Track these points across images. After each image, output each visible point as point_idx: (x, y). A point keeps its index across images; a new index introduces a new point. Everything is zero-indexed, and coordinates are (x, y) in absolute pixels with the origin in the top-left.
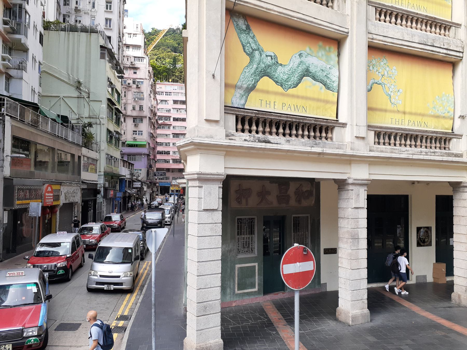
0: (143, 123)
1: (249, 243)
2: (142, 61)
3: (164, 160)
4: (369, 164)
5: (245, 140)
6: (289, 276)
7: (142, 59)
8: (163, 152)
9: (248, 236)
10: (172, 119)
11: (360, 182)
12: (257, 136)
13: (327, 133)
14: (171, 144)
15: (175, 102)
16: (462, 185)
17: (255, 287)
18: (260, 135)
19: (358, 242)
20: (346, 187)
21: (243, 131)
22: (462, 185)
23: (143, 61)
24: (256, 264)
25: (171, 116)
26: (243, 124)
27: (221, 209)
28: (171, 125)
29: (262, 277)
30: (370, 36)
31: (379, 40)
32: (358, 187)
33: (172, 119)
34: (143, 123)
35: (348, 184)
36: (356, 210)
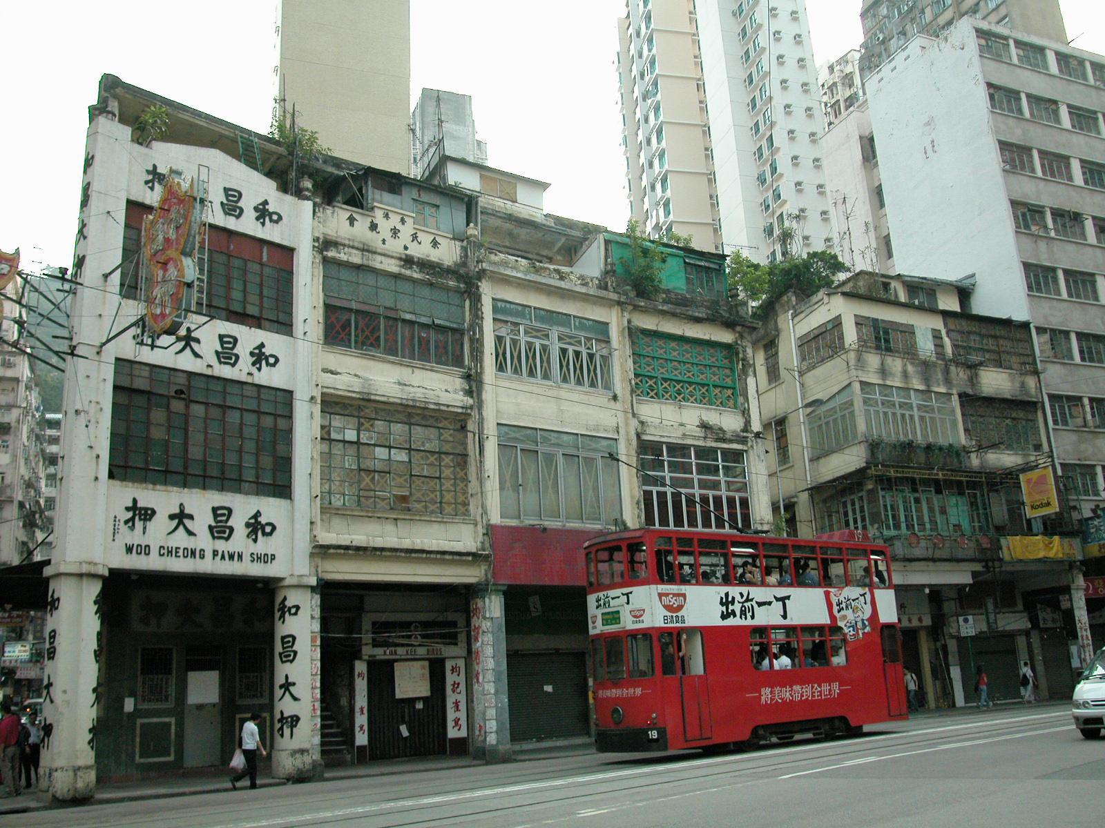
1: (161, 688)
9: (160, 676)
17: (169, 755)
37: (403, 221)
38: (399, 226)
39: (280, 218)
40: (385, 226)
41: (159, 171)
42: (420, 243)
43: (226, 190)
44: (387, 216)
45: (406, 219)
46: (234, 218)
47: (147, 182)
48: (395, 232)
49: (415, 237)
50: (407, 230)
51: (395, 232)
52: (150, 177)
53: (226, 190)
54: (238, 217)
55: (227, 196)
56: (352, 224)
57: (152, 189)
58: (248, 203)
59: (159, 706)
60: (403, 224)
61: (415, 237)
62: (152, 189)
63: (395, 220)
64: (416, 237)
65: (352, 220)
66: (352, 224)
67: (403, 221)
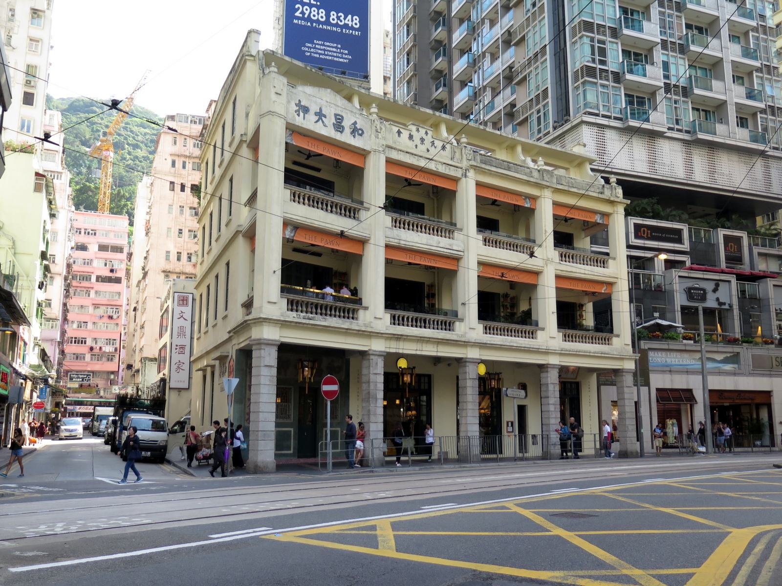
0: (52, 285)
2: (57, 179)
3: (74, 354)
4: (385, 340)
5: (294, 317)
6: (326, 392)
7: (58, 176)
8: (74, 340)
10: (94, 278)
11: (378, 353)
12: (302, 314)
13: (353, 314)
14: (89, 324)
15: (103, 248)
16: (463, 360)
17: (290, 450)
18: (304, 314)
19: (376, 400)
20: (368, 357)
21: (292, 310)
22: (463, 360)
23: (60, 179)
24: (292, 430)
25: (93, 273)
26: (292, 306)
27: (276, 366)
28: (92, 288)
29: (297, 442)
30: (387, 239)
31: (394, 242)
32: (376, 357)
33: (94, 278)
34: (52, 285)
35: (369, 354)
36: (375, 376)
37: (426, 133)
38: (424, 136)
39: (363, 132)
40: (417, 136)
41: (302, 104)
42: (435, 147)
43: (336, 115)
44: (418, 130)
45: (428, 132)
46: (339, 133)
47: (296, 112)
48: (422, 140)
49: (433, 143)
50: (428, 139)
51: (422, 140)
52: (298, 108)
53: (336, 115)
54: (341, 132)
55: (336, 119)
56: (399, 135)
57: (299, 115)
58: (347, 123)
59: (285, 421)
60: (427, 135)
61: (433, 143)
62: (299, 115)
63: (422, 131)
64: (434, 144)
65: (399, 133)
66: (399, 135)
67: (426, 133)
